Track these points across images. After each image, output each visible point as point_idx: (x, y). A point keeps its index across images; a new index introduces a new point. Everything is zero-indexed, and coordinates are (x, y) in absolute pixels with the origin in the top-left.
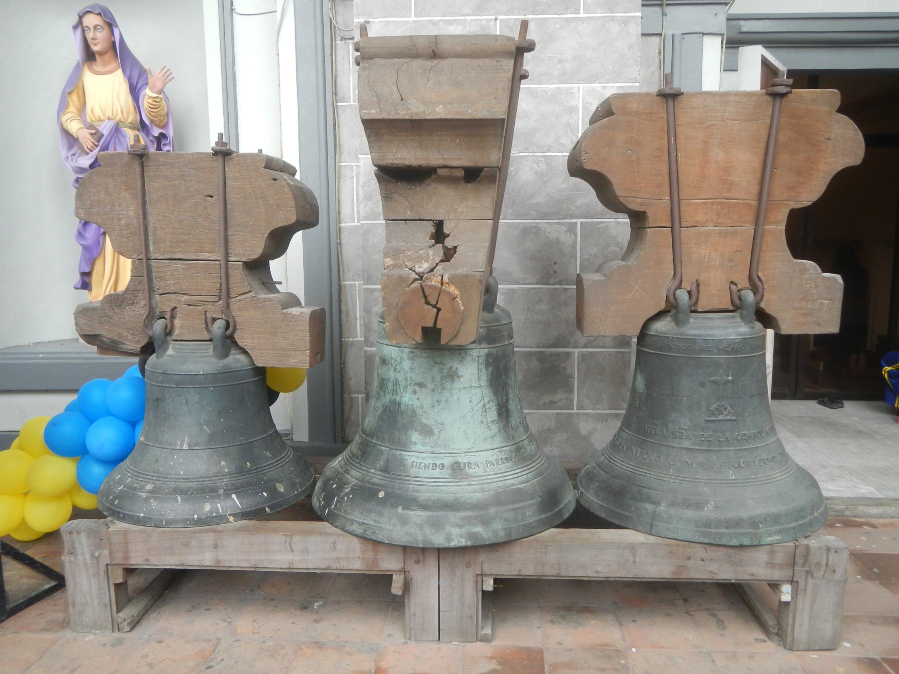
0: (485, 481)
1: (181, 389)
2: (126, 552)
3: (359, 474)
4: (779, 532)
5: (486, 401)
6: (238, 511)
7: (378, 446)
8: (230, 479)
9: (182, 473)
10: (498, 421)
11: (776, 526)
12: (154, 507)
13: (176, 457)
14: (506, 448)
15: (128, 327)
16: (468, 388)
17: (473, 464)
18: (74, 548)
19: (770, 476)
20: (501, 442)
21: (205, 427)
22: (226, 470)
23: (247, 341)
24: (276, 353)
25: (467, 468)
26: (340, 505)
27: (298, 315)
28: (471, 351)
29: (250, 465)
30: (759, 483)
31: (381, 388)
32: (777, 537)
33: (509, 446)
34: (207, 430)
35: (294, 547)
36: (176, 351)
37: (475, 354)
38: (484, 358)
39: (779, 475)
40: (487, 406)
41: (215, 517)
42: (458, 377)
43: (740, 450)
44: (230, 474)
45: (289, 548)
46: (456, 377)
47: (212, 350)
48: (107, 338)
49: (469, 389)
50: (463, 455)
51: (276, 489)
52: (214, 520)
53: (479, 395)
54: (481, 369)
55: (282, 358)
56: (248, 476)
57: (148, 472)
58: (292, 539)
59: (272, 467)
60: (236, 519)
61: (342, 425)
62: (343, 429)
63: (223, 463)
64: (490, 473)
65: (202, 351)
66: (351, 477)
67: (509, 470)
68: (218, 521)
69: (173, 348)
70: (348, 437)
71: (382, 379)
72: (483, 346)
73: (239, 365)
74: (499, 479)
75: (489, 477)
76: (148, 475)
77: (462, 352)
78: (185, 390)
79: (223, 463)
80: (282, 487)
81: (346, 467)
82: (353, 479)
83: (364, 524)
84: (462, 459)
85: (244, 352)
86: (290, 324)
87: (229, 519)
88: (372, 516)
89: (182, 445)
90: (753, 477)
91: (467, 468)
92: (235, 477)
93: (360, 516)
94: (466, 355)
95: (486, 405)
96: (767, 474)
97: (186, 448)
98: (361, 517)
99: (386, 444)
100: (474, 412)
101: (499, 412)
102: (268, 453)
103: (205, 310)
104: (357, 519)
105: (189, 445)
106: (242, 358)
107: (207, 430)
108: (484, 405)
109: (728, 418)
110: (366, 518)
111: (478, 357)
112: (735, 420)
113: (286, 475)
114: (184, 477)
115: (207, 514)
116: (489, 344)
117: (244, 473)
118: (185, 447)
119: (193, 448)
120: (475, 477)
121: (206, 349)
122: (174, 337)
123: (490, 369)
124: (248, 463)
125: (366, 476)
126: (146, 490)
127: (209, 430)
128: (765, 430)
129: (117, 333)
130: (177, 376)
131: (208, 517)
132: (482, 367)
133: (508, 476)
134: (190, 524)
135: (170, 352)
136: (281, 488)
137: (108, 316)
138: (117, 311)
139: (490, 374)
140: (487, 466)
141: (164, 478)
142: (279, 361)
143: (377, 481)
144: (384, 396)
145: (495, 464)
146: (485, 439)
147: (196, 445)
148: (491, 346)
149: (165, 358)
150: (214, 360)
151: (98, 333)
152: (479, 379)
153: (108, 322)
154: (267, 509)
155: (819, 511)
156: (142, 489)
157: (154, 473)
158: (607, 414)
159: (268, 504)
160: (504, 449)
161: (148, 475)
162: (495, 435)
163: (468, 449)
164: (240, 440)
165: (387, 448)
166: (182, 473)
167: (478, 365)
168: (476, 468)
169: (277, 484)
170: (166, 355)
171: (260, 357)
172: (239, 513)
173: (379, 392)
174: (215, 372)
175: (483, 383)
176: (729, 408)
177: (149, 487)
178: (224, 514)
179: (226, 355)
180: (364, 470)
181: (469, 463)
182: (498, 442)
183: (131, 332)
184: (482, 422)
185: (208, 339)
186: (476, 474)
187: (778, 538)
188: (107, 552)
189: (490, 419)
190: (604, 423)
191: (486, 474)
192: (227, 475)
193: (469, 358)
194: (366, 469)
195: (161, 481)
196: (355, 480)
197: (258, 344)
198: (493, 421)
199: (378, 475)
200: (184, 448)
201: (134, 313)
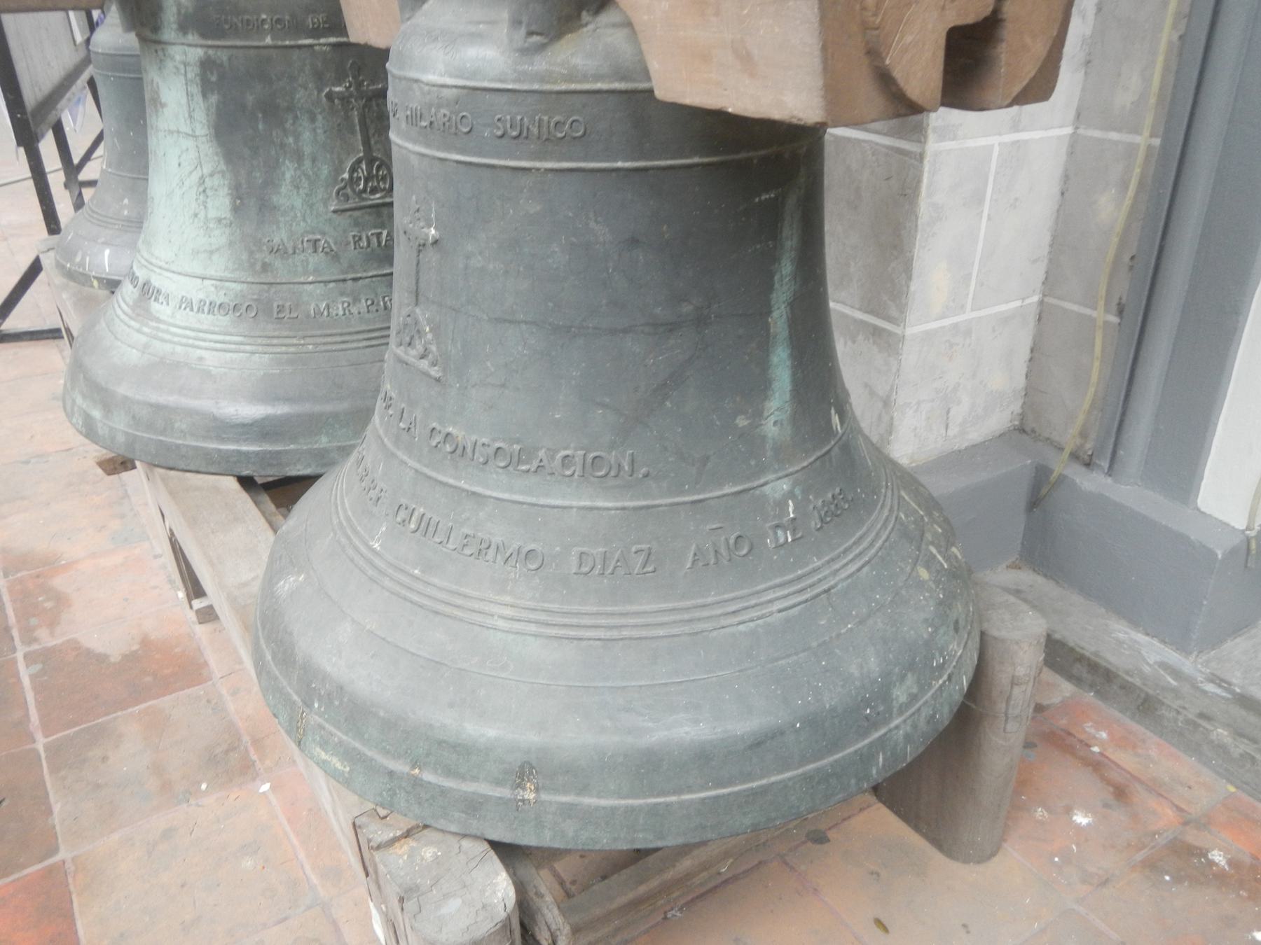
0: (160, 334)
4: (349, 755)
5: (207, 169)
6: (104, 276)
10: (231, 224)
11: (346, 734)
14: (233, 285)
17: (164, 294)
19: (465, 596)
20: (227, 268)
22: (126, 213)
25: (153, 298)
30: (416, 598)
32: (339, 766)
33: (248, 283)
34: (118, 146)
37: (178, 58)
38: (197, 70)
39: (508, 612)
40: (208, 182)
41: (81, 273)
42: (161, 103)
43: (429, 478)
44: (128, 221)
46: (159, 105)
50: (158, 270)
53: (192, 154)
54: (192, 96)
63: (126, 201)
64: (178, 322)
67: (217, 329)
74: (184, 341)
75: (173, 329)
77: (159, 47)
79: (126, 201)
84: (156, 282)
87: (93, 283)
90: (416, 572)
91: (153, 298)
94: (165, 55)
95: (207, 180)
96: (463, 590)
100: (184, 189)
101: (238, 201)
108: (202, 180)
109: (424, 364)
111: (185, 64)
112: (438, 380)
116: (204, 35)
120: (152, 320)
123: (214, 99)
128: (541, 454)
132: (196, 90)
133: (204, 340)
139: (213, 110)
140: (180, 307)
145: (195, 309)
146: (196, 253)
148: (210, 42)
152: (190, 117)
155: (544, 797)
158: (855, 321)
160: (227, 284)
162: (218, 250)
163: (167, 263)
167: (186, 84)
168: (165, 303)
172: (104, 279)
175: (202, 130)
176: (430, 336)
181: (159, 292)
182: (219, 265)
184: (196, 215)
186: (158, 315)
187: (339, 766)
189: (212, 213)
190: (849, 343)
191: (171, 321)
193: (170, 65)
198: (219, 220)
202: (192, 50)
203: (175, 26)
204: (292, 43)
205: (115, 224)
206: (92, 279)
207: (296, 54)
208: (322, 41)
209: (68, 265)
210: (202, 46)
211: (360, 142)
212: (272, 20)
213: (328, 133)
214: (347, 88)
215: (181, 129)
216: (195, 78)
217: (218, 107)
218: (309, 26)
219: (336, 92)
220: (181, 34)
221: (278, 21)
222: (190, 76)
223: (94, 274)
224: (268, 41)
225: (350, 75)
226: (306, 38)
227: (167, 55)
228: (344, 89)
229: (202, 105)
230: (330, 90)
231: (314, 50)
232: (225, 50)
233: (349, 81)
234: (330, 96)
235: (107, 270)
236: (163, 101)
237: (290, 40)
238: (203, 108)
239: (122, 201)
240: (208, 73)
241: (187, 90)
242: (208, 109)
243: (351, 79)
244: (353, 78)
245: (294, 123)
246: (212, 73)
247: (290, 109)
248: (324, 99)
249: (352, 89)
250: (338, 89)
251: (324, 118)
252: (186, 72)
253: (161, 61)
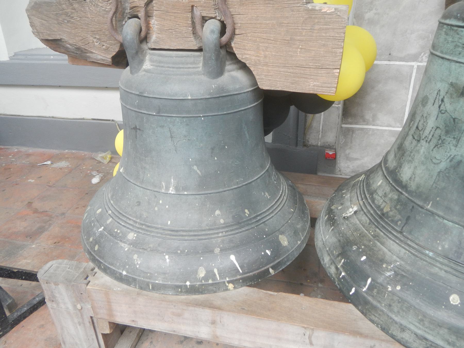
1: (164, 118)
2: (110, 311)
3: (404, 251)
6: (239, 277)
7: (437, 217)
8: (227, 234)
9: (169, 223)
12: (138, 266)
13: (161, 202)
15: (93, 29)
18: (54, 297)
21: (195, 168)
22: (222, 221)
23: (249, 52)
24: (289, 70)
26: (378, 293)
27: (330, 14)
29: (248, 213)
31: (447, 132)
34: (198, 171)
35: (314, 341)
36: (155, 64)
41: (212, 285)
45: (307, 341)
47: (201, 65)
48: (70, 45)
51: (279, 244)
52: (211, 288)
55: (297, 79)
56: (247, 228)
57: (130, 215)
58: (313, 333)
59: (272, 212)
60: (236, 286)
61: (304, 131)
62: (304, 134)
63: (218, 212)
65: (189, 66)
66: (389, 251)
68: (214, 289)
69: (151, 60)
70: (308, 141)
71: (454, 119)
73: (238, 87)
76: (130, 219)
78: (169, 119)
79: (218, 212)
80: (286, 239)
81: (375, 231)
82: (395, 257)
83: (426, 339)
85: (244, 67)
86: (317, 27)
87: (228, 286)
88: (441, 332)
89: (167, 188)
92: (231, 231)
93: (417, 324)
97: (173, 193)
98: (421, 327)
99: (455, 218)
102: (267, 194)
103: (192, 4)
104: (412, 327)
105: (176, 189)
106: (240, 75)
107: (198, 171)
110: (431, 332)
113: (287, 222)
114: (173, 228)
115: (201, 281)
117: (242, 224)
118: (172, 191)
119: (181, 193)
121: (194, 63)
122: (151, 44)
124: (246, 211)
125: (417, 259)
126: (128, 240)
127: (201, 171)
129: (81, 38)
130: (157, 101)
131: (203, 285)
134: (181, 292)
135: (147, 65)
136: (284, 241)
137: (66, 14)
138: (76, 6)
141: (148, 226)
142: (292, 84)
143: (442, 274)
144: (456, 146)
147: (185, 189)
149: (141, 73)
150: (205, 78)
151: (58, 37)
153: (68, 22)
154: (271, 270)
156: (123, 238)
157: (137, 217)
159: (272, 265)
161: (130, 219)
164: (237, 182)
165: (457, 226)
166: (169, 223)
169: (280, 236)
170: (142, 69)
171: (266, 76)
173: (443, 137)
174: (208, 97)
177: (131, 236)
178: (222, 281)
179: (220, 72)
180: (414, 248)
183: (97, 37)
185: (196, 48)
188: (89, 306)
192: (223, 228)
194: (416, 247)
195: (144, 229)
196: (398, 260)
197: (265, 57)
199: (442, 263)
200: (170, 192)
201: (98, 9)
205: (218, 233)
206: (227, 285)
209: (188, 283)
223: (227, 279)
235: (241, 272)
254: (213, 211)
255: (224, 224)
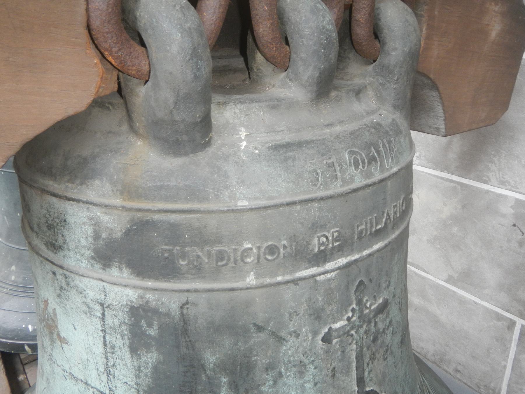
16: (80, 382)
21: (5, 218)
22: (13, 278)
28: (77, 278)
34: (8, 223)
49: (81, 385)
54: (113, 347)
63: (13, 268)
72: (115, 273)
79: (13, 268)
111: (102, 305)
148: (150, 284)
167: (104, 331)
202: (116, 289)
203: (89, 253)
204: (288, 277)
205: (4, 288)
207: (288, 293)
208: (329, 266)
210: (135, 287)
211: (355, 383)
212: (259, 248)
213: (318, 385)
214: (349, 319)
215: (89, 382)
216: (120, 325)
217: (155, 368)
218: (313, 250)
219: (337, 330)
220: (98, 266)
221: (272, 250)
222: (110, 322)
224: (251, 280)
225: (355, 302)
226: (307, 268)
227: (72, 284)
228: (346, 323)
229: (129, 361)
230: (330, 328)
231: (316, 280)
232: (177, 294)
233: (353, 310)
234: (326, 339)
236: (63, 334)
237: (283, 275)
238: (130, 367)
239: (10, 267)
240: (143, 323)
241: (104, 338)
242: (139, 369)
243: (354, 306)
244: (356, 305)
245: (275, 382)
246: (150, 325)
247: (269, 368)
248: (320, 342)
249: (354, 318)
250: (337, 325)
251: (315, 368)
252: (103, 315)
253: (61, 288)
254: (11, 265)
255: (13, 281)
